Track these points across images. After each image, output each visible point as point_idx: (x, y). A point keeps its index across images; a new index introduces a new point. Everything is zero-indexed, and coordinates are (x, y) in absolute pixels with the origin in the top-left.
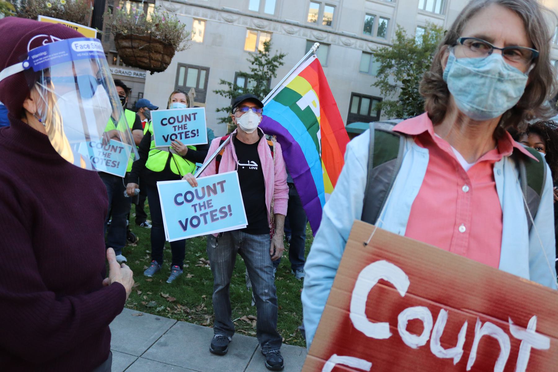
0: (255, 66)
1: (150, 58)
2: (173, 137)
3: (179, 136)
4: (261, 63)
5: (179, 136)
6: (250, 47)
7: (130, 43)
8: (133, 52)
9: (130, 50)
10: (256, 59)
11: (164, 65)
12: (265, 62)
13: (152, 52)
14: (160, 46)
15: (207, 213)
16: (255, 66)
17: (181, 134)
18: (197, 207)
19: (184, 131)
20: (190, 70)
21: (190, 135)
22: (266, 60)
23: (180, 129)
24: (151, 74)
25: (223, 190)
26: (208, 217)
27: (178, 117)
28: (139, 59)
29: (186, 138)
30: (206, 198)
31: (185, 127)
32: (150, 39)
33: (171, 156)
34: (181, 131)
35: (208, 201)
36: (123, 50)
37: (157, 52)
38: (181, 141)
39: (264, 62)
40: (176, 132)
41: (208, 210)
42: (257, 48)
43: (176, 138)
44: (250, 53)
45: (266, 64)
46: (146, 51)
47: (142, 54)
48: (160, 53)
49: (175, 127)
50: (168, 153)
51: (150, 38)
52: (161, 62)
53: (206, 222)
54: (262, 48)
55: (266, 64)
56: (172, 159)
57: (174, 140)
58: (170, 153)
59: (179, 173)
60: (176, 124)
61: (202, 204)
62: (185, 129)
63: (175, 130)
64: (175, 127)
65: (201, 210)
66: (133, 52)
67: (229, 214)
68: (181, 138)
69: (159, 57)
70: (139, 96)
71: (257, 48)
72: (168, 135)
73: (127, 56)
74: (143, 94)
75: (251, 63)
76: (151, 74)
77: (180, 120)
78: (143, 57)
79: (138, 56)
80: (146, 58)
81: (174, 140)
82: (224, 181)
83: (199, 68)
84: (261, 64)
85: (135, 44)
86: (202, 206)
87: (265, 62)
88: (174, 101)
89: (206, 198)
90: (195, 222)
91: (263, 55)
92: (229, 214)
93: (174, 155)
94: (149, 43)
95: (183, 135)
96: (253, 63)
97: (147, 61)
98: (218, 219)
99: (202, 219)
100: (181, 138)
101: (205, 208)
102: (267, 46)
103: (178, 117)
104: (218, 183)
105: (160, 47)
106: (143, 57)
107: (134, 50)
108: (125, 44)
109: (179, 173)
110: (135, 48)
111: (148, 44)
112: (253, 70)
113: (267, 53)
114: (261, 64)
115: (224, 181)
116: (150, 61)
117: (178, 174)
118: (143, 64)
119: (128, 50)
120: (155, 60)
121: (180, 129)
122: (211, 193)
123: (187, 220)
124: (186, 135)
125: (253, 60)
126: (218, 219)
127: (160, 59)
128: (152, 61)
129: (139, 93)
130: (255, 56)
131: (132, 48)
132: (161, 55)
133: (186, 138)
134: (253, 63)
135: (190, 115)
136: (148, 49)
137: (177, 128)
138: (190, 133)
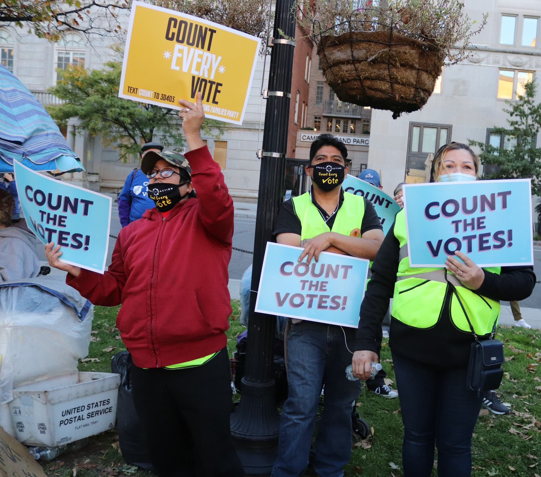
0: (515, 118)
1: (393, 80)
2: (452, 247)
3: (464, 244)
4: (524, 113)
5: (464, 244)
6: (505, 92)
7: (349, 52)
8: (356, 70)
9: (350, 67)
10: (516, 109)
11: (422, 94)
12: (529, 111)
13: (395, 66)
14: (413, 51)
16: (515, 118)
17: (469, 239)
19: (478, 232)
20: (426, 131)
21: (492, 242)
22: (530, 109)
23: (469, 228)
24: (395, 117)
27: (464, 200)
28: (368, 83)
29: (481, 248)
31: (479, 223)
32: (388, 38)
33: (451, 290)
34: (469, 232)
36: (336, 69)
37: (406, 65)
38: (469, 255)
39: (527, 111)
40: (460, 236)
42: (515, 92)
43: (459, 248)
44: (506, 101)
45: (531, 114)
46: (384, 66)
47: (375, 71)
48: (412, 67)
49: (456, 223)
50: (444, 285)
51: (391, 34)
52: (417, 89)
54: (522, 91)
55: (531, 114)
56: (454, 296)
57: (452, 253)
58: (449, 284)
59: (472, 328)
60: (460, 216)
62: (479, 228)
63: (457, 230)
64: (456, 223)
66: (356, 70)
68: (470, 250)
69: (410, 75)
70: (361, 168)
71: (515, 92)
72: (440, 242)
73: (343, 82)
74: (366, 165)
75: (509, 115)
76: (395, 117)
77: (469, 207)
78: (378, 78)
79: (367, 78)
80: (383, 80)
81: (452, 253)
83: (438, 127)
84: (523, 114)
85: (360, 53)
87: (529, 111)
88: (449, 166)
91: (525, 102)
93: (459, 288)
94: (390, 46)
95: (475, 243)
96: (512, 115)
97: (385, 86)
100: (470, 250)
102: (530, 88)
103: (464, 200)
105: (411, 54)
106: (378, 78)
107: (357, 65)
108: (339, 54)
109: (472, 328)
110: (359, 61)
111: (386, 50)
112: (512, 124)
113: (530, 98)
114: (523, 114)
116: (392, 87)
117: (469, 330)
118: (379, 95)
119: (345, 68)
120: (403, 84)
121: (469, 228)
124: (481, 242)
125: (511, 109)
127: (413, 81)
128: (397, 86)
129: (362, 165)
130: (514, 104)
131: (354, 61)
132: (414, 72)
133: (481, 248)
134: (512, 115)
135: (493, 196)
136: (387, 61)
137: (461, 226)
138: (491, 239)
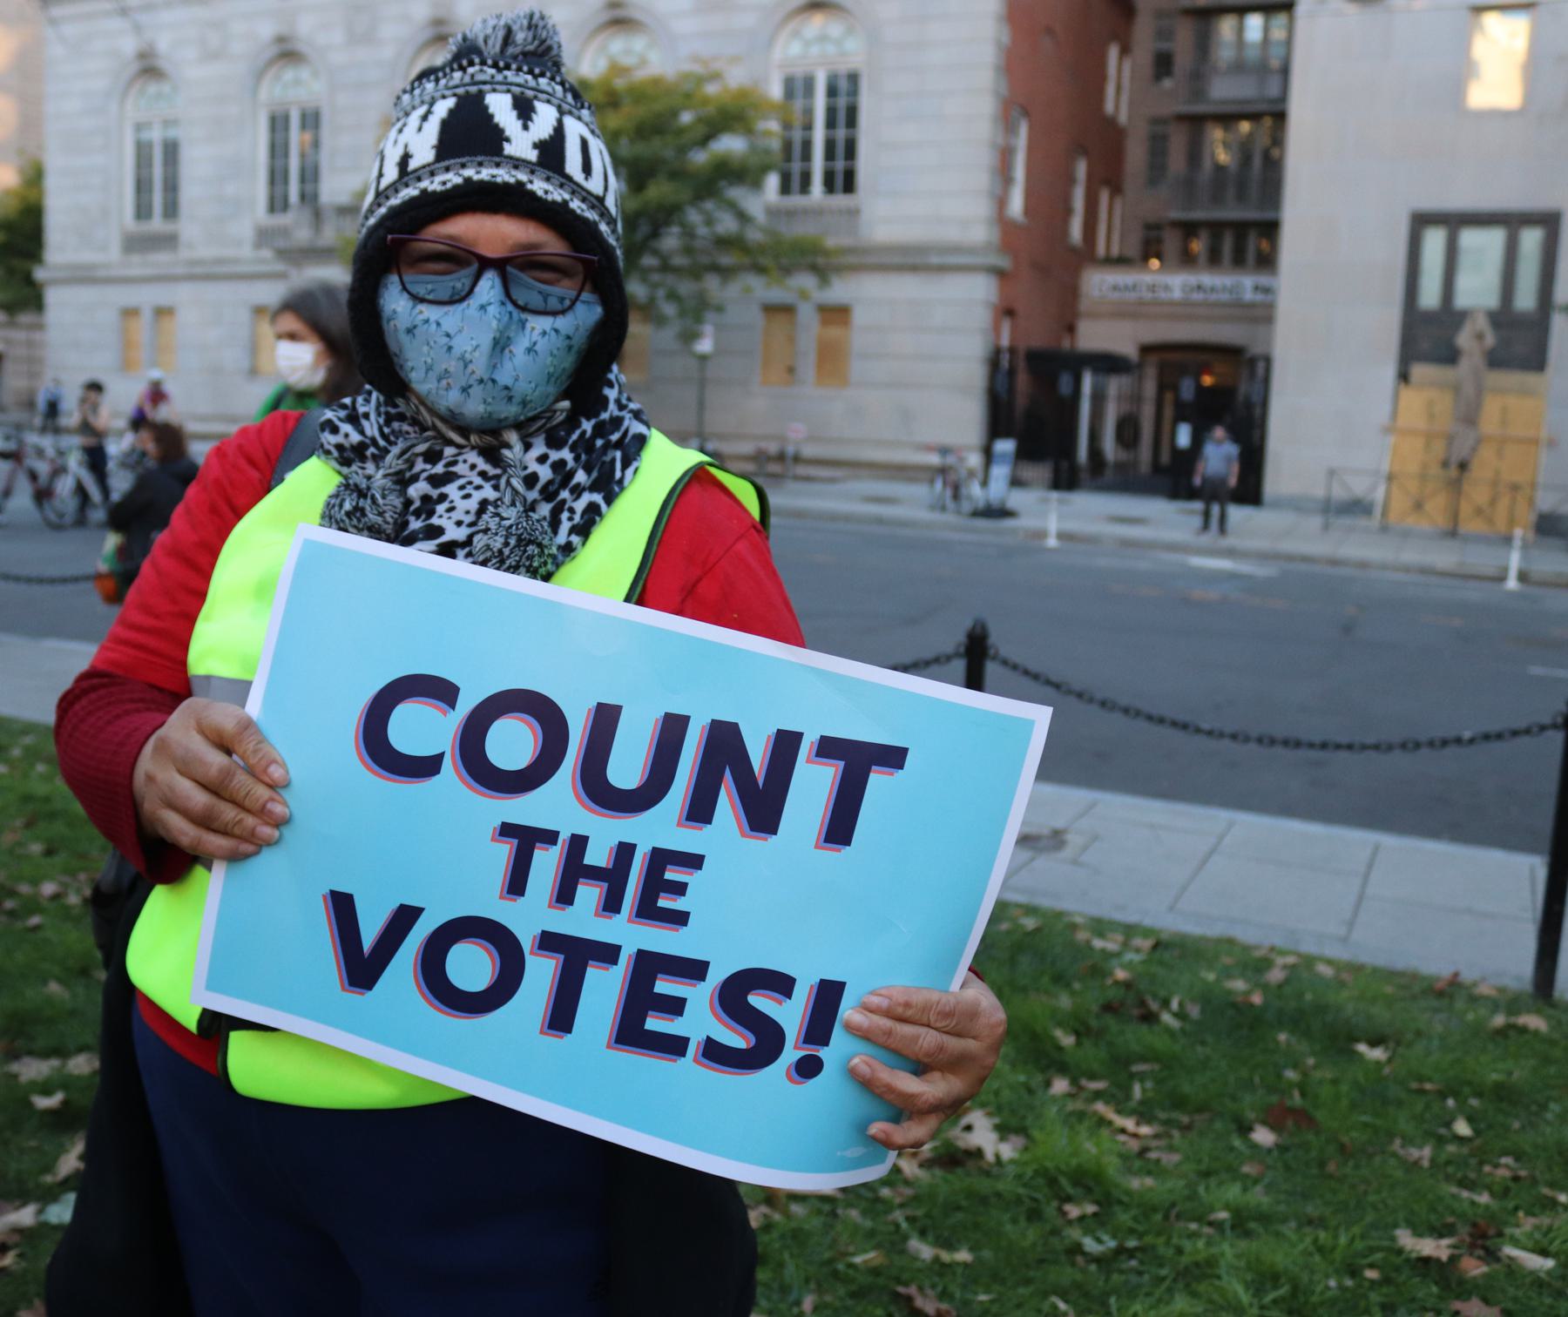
15: (609, 953)
18: (546, 864)
25: (840, 829)
26: (603, 991)
30: (661, 827)
35: (661, 859)
41: (631, 935)
53: (561, 1017)
61: (597, 856)
65: (565, 896)
67: (791, 1054)
82: (893, 757)
86: (595, 873)
89: (661, 827)
90: (471, 966)
92: (791, 1054)
98: (674, 1046)
99: (541, 973)
101: (611, 905)
104: (828, 748)
115: (893, 757)
122: (726, 806)
123: (405, 917)
126: (674, 1046)
